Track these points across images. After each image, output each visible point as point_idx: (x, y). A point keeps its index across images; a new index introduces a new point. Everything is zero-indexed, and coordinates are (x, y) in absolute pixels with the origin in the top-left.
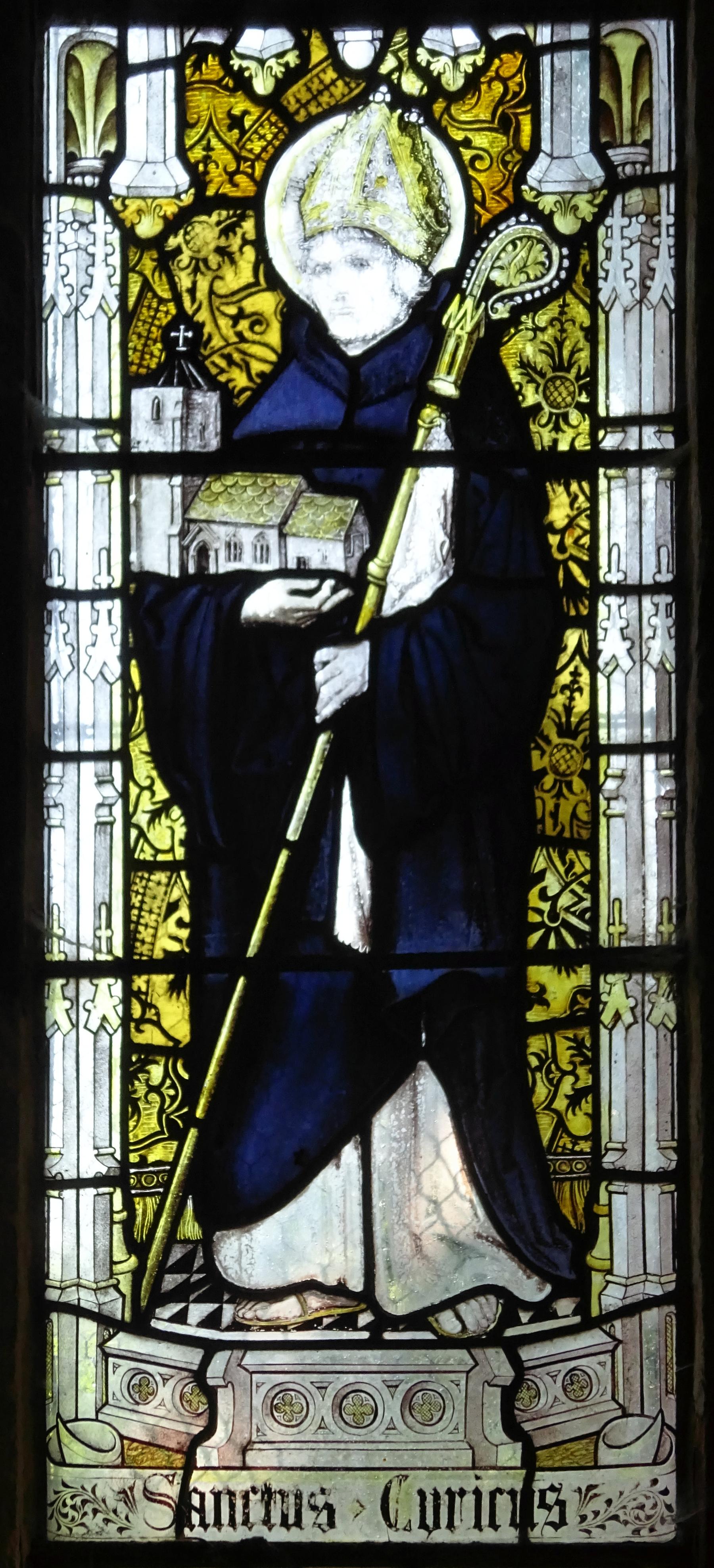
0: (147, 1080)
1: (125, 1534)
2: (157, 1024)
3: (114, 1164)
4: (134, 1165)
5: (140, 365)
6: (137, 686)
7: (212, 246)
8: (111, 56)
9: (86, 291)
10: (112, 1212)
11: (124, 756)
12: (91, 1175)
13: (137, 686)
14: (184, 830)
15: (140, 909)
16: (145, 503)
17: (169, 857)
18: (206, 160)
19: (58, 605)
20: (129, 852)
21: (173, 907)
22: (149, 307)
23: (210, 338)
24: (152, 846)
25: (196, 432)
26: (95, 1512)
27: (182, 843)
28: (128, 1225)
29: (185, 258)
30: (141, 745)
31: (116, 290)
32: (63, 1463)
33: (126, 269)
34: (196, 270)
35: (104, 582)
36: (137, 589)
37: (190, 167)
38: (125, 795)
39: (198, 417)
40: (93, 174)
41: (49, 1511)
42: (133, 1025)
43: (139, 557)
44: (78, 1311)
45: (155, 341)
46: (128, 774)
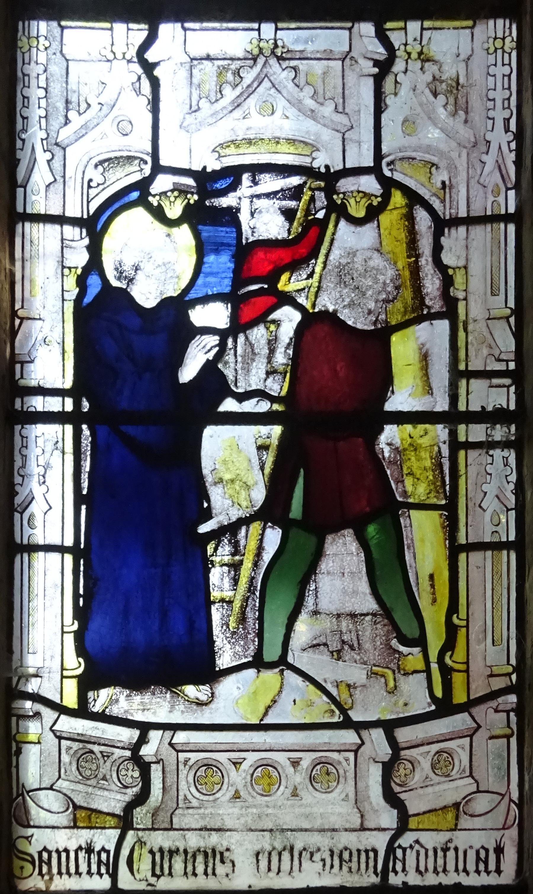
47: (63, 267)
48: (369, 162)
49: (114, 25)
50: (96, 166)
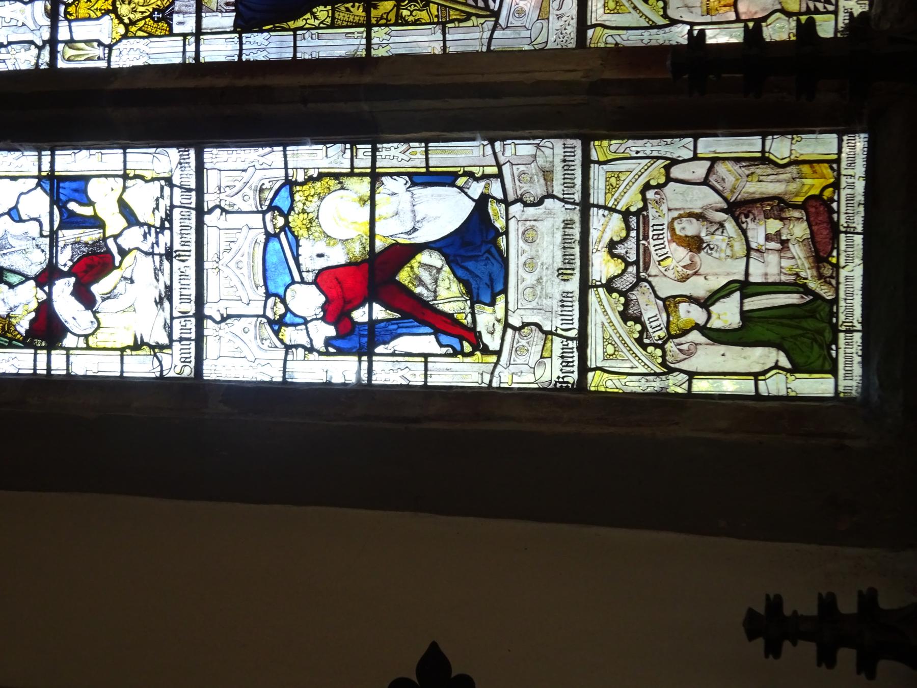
0: (409, 16)
1: (574, 17)
2: (388, 13)
3: (438, 27)
4: (438, 19)
5: (166, 30)
6: (272, 26)
7: (127, 6)
8: (68, 46)
9: (142, 51)
10: (455, 27)
11: (295, 30)
12: (442, 36)
13: (272, 26)
14: (321, 7)
15: (348, 22)
16: (211, 26)
17: (330, 12)
18: (101, 10)
19: (244, 58)
20: (328, 27)
21: (348, 10)
22: (147, 28)
23: (158, 5)
24: (326, 18)
25: (188, 9)
26: (565, 29)
27: (325, 7)
28: (460, 21)
29: (132, 16)
30: (292, 24)
31: (142, 40)
32: (547, 42)
33: (135, 37)
34: (135, 11)
35: (237, 40)
36: (239, 28)
37: (103, 15)
38: (308, 29)
39: (183, 8)
40: (104, 50)
41: (564, 47)
42: (388, 23)
43: (229, 28)
44: (491, 38)
45: (158, 25)
46: (302, 28)
47: (304, 360)
48: (261, 215)
49: (205, 334)
50: (263, 344)
